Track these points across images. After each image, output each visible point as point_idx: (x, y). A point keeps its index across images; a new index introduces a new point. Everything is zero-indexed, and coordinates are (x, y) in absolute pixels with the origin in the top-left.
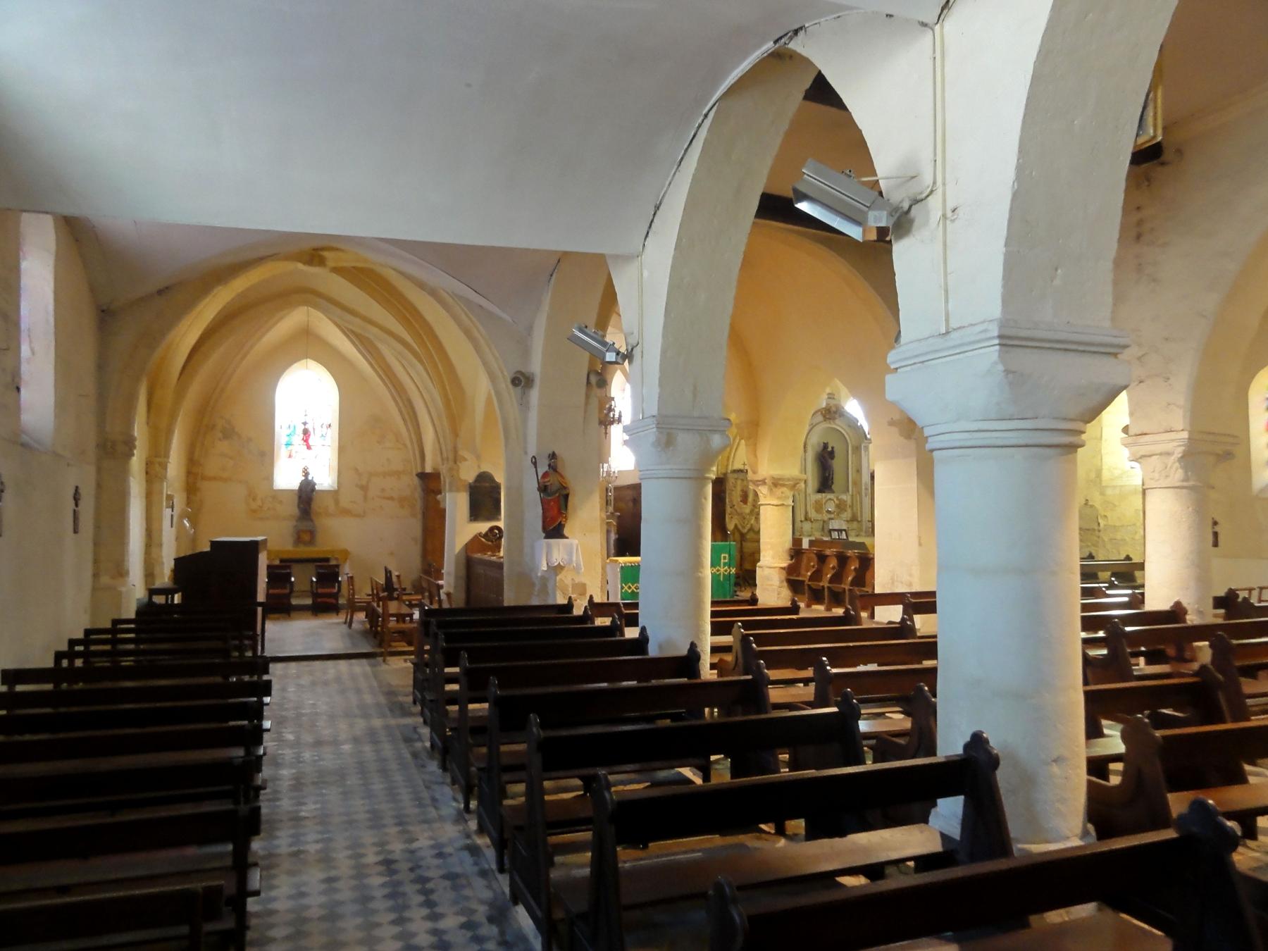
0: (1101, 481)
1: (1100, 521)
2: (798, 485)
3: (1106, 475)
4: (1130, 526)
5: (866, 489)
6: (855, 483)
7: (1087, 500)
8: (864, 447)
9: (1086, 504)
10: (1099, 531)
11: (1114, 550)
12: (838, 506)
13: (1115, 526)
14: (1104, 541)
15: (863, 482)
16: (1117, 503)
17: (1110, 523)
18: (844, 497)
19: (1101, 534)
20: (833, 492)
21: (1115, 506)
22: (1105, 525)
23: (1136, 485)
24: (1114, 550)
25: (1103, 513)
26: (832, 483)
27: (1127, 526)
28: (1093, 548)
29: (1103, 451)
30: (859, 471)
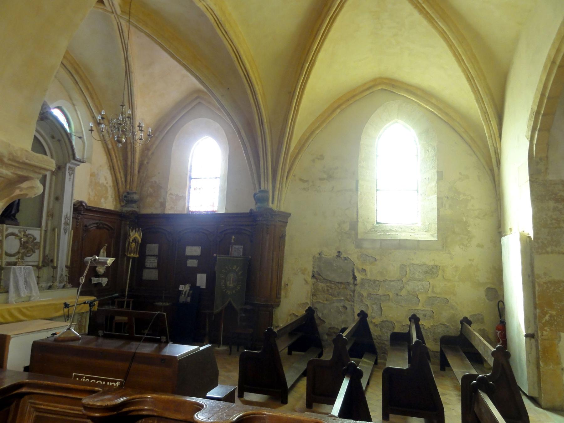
0: (357, 234)
1: (357, 274)
2: (25, 185)
3: (361, 228)
4: (393, 281)
5: (66, 224)
6: (51, 215)
7: (339, 252)
8: (70, 168)
9: (338, 256)
10: (356, 285)
11: (374, 306)
12: (23, 245)
13: (375, 281)
14: (361, 295)
15: (64, 214)
16: (378, 258)
17: (369, 277)
18: (36, 233)
19: (358, 288)
20: (17, 224)
21: (376, 260)
22: (362, 279)
23: (400, 240)
24: (374, 306)
25: (360, 267)
26: (18, 211)
27: (391, 281)
28: (346, 302)
29: (359, 204)
30: (58, 199)
